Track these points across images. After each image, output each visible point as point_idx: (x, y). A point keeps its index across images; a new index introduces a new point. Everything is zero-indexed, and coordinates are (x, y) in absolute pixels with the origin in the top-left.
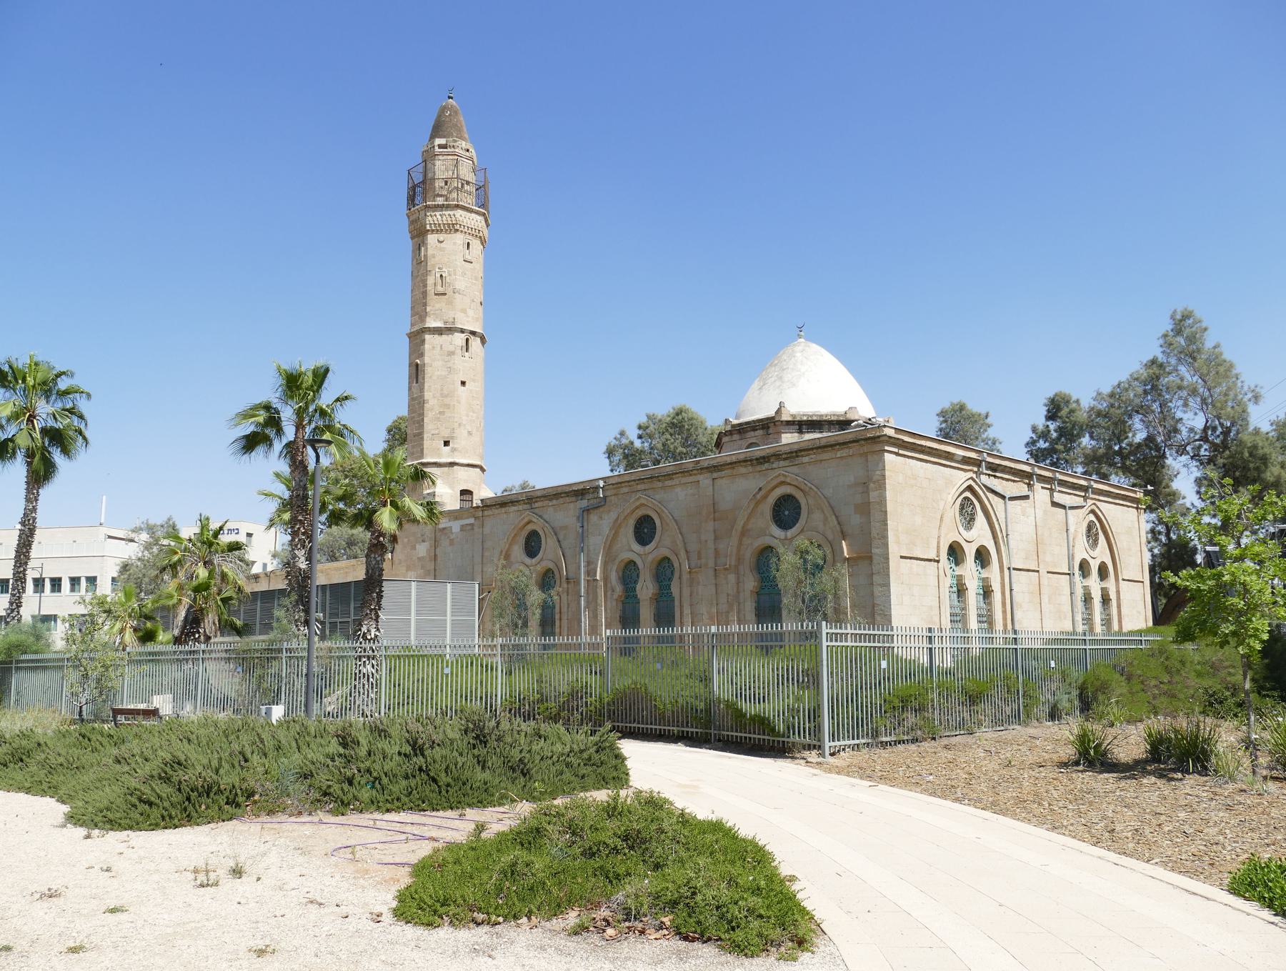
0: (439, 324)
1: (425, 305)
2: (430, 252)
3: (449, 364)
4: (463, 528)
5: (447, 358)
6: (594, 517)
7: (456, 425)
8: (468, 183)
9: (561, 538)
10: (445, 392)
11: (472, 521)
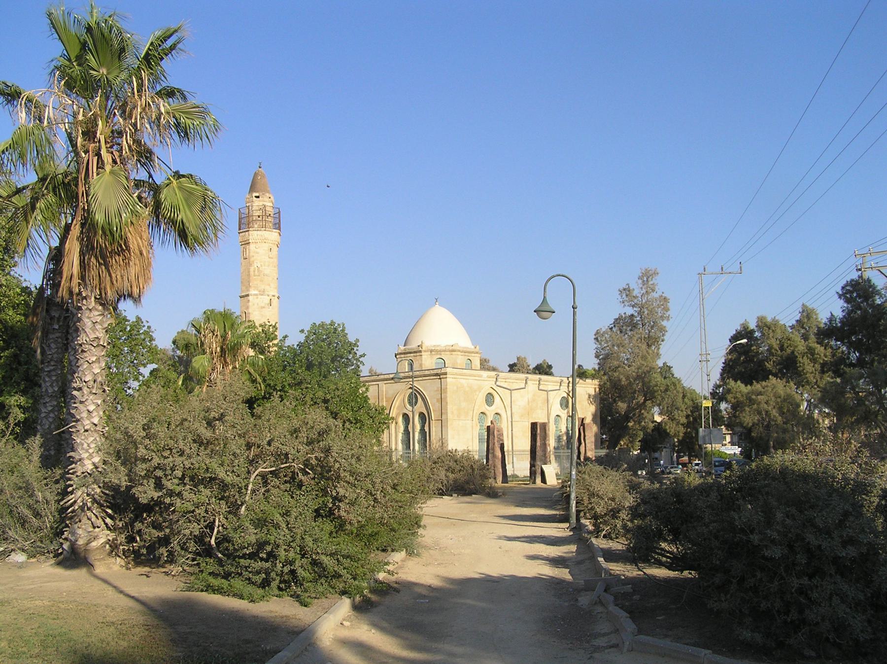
0: (256, 292)
1: (249, 282)
2: (251, 254)
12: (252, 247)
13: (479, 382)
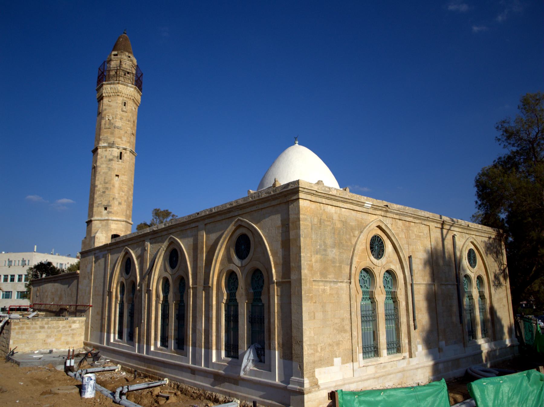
0: (106, 145)
1: (100, 135)
2: (104, 107)
3: (110, 166)
5: (108, 163)
7: (111, 199)
8: (128, 73)
10: (106, 181)
12: (105, 101)
13: (359, 215)
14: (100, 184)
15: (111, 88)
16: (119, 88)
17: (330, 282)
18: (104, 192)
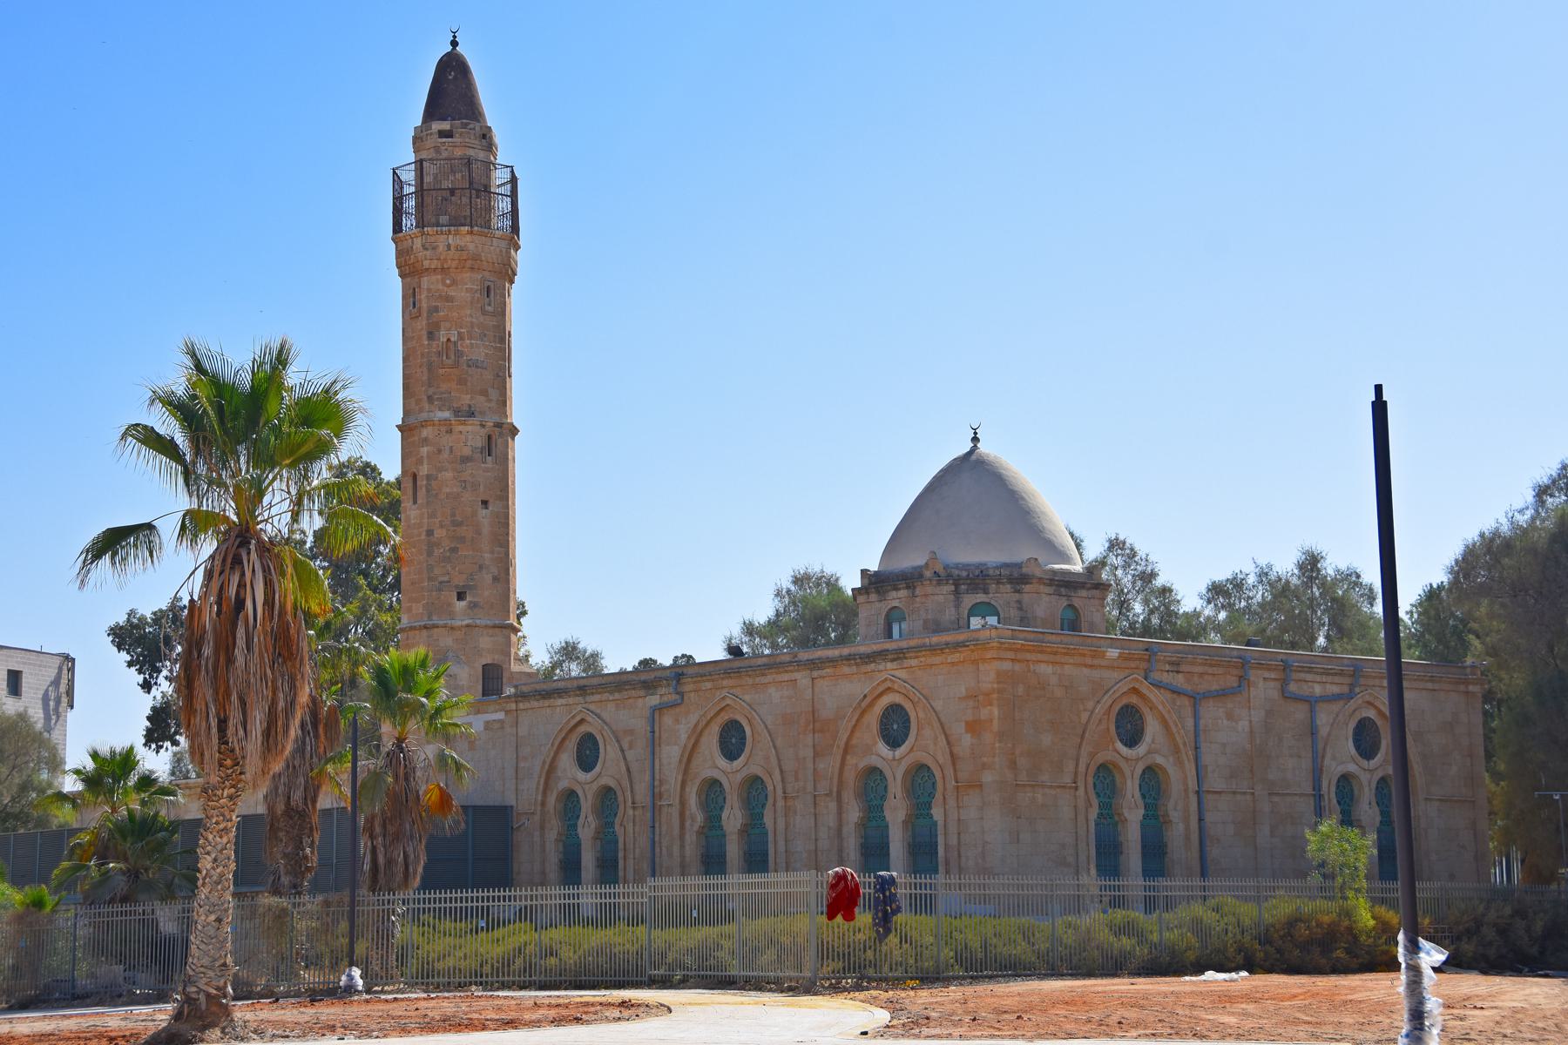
4: (488, 725)
6: (668, 720)
9: (626, 746)
11: (500, 716)
13: (1096, 674)
14: (442, 526)
15: (449, 246)
16: (471, 247)
17: (1043, 787)
18: (454, 550)
